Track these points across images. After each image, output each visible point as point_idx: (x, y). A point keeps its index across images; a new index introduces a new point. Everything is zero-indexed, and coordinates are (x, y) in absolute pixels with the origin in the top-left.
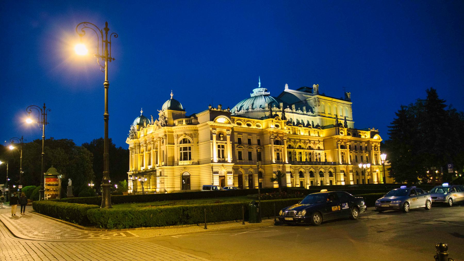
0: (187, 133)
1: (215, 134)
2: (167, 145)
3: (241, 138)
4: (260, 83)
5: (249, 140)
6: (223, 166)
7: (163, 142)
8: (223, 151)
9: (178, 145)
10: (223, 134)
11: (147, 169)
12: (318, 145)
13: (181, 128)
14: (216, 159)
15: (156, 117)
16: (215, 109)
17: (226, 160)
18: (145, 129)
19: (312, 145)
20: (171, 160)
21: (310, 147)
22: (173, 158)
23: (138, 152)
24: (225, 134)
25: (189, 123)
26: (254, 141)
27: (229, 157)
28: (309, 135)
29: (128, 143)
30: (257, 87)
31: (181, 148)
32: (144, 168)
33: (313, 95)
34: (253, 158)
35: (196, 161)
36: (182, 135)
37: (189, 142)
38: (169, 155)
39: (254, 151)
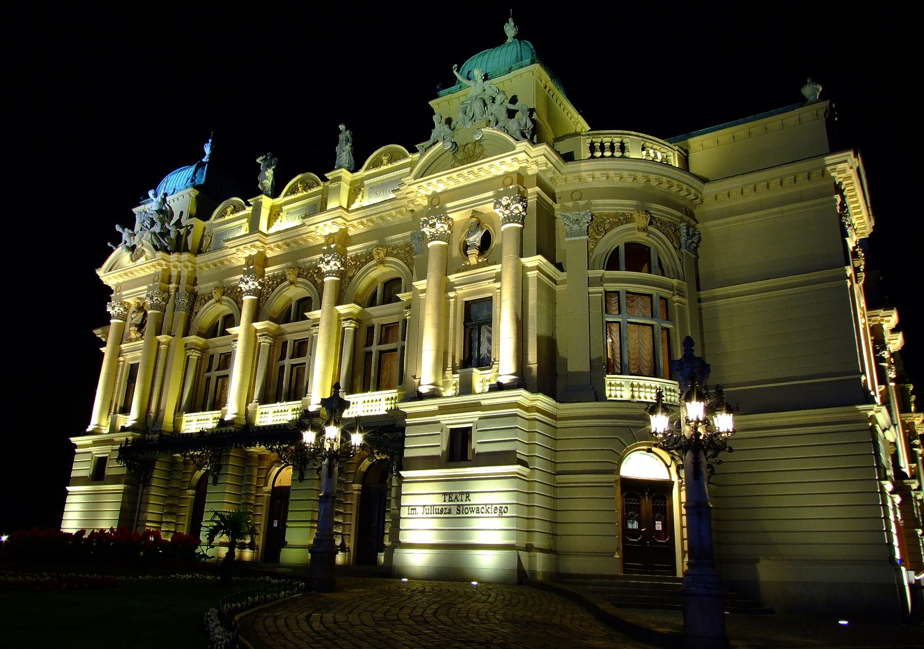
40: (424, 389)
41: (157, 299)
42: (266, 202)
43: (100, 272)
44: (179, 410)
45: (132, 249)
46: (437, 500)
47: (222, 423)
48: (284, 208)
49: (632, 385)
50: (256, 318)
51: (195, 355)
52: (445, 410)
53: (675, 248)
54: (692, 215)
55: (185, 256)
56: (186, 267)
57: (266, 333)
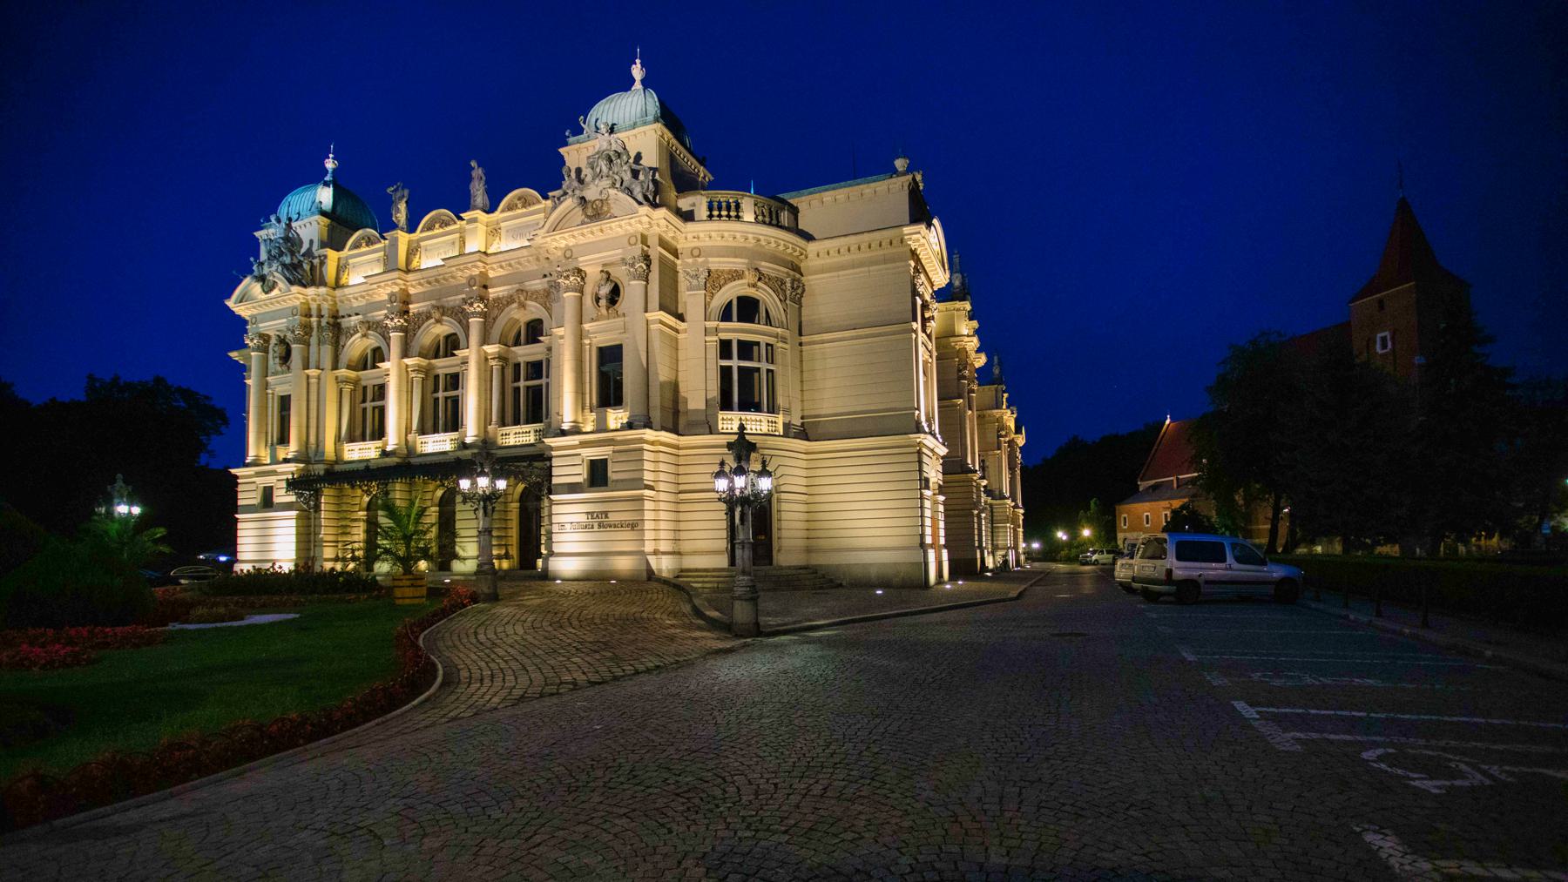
0: (766, 267)
13: (723, 239)
25: (770, 219)
29: (242, 310)
37: (769, 321)
40: (565, 427)
42: (403, 238)
43: (230, 303)
44: (338, 439)
45: (262, 279)
46: (583, 518)
47: (384, 454)
51: (347, 388)
52: (584, 444)
54: (796, 269)
55: (323, 290)
57: (419, 369)
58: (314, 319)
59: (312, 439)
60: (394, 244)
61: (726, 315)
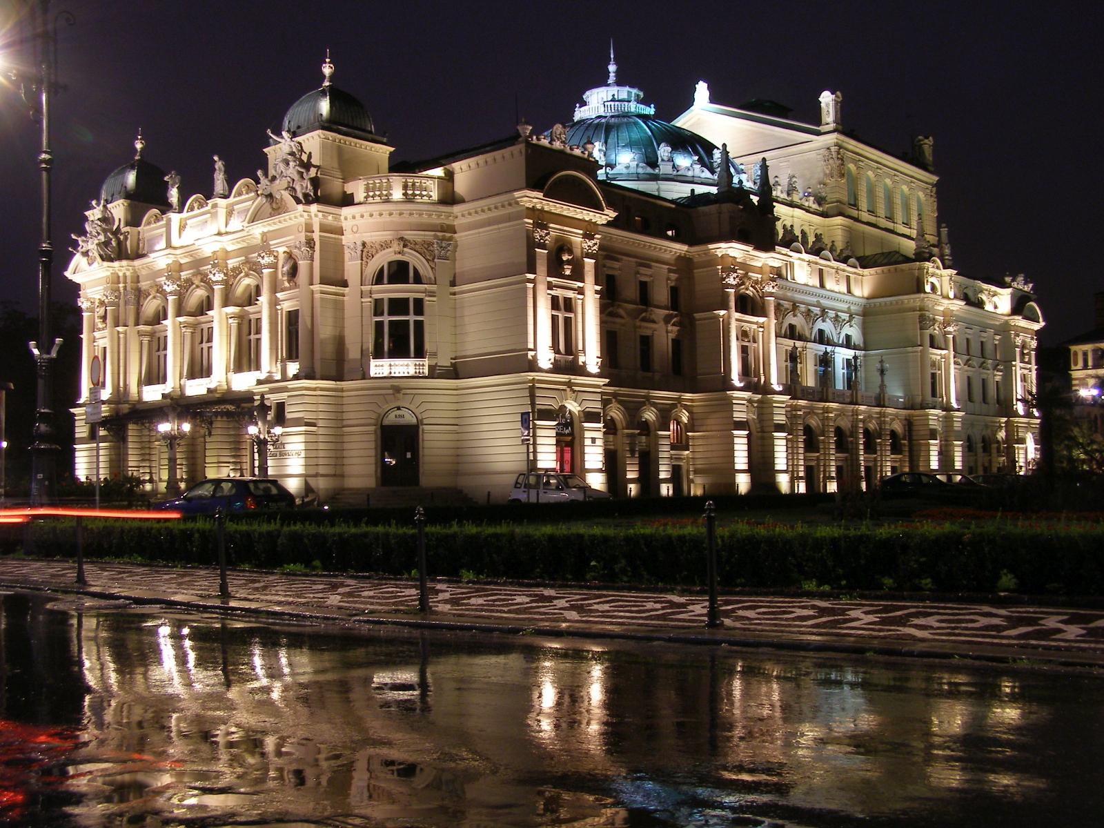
0: (409, 235)
1: (543, 246)
2: (317, 287)
3: (616, 273)
4: (612, 68)
5: (644, 287)
6: (569, 384)
7: (293, 272)
8: (568, 321)
9: (366, 288)
10: (570, 252)
11: (182, 395)
12: (847, 330)
14: (545, 357)
15: (248, 164)
16: (545, 142)
17: (581, 359)
18: (175, 218)
19: (827, 327)
20: (330, 349)
21: (821, 332)
22: (340, 342)
23: (131, 321)
24: (577, 252)
26: (661, 294)
27: (591, 358)
28: (822, 286)
29: (76, 279)
30: (602, 82)
31: (378, 303)
32: (167, 388)
33: (818, 133)
34: (657, 362)
35: (445, 362)
36: (385, 245)
37: (418, 279)
38: (325, 331)
39: (664, 334)
41: (112, 298)
43: (68, 274)
44: (140, 384)
48: (188, 222)
49: (390, 365)
50: (179, 313)
53: (427, 260)
55: (124, 263)
56: (128, 270)
57: (187, 325)
58: (121, 285)
59: (122, 384)
60: (169, 221)
61: (379, 279)
